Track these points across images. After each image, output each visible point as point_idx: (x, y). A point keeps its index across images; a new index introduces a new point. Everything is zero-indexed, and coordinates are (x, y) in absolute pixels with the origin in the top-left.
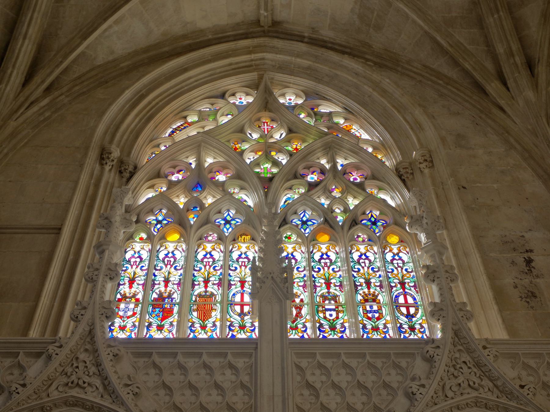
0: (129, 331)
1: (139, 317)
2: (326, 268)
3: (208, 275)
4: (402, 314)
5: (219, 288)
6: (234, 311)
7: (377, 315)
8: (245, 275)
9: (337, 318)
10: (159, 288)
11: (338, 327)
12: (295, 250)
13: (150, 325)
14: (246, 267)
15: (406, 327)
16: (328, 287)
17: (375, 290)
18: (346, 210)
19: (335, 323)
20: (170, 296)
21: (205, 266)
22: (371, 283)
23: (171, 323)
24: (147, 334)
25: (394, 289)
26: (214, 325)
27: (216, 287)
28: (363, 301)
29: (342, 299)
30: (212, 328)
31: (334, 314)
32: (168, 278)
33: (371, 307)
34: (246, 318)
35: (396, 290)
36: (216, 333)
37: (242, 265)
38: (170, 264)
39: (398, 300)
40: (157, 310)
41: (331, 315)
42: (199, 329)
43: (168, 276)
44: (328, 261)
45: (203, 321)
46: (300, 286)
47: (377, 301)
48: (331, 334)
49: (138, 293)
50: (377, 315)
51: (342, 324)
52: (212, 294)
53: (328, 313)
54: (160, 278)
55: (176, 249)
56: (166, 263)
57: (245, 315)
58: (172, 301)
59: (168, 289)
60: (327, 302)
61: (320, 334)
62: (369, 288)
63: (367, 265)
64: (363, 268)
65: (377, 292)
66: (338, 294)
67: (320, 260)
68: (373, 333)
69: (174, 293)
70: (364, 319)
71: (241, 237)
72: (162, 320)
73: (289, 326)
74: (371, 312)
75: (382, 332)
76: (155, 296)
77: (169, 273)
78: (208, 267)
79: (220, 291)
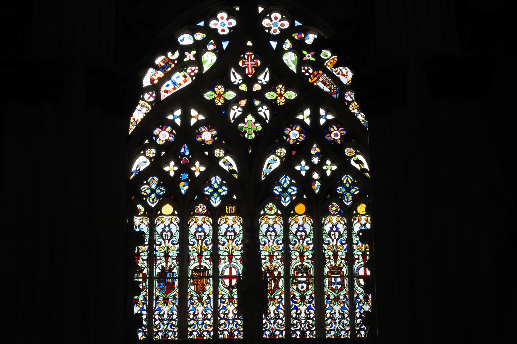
0: (141, 304)
1: (147, 291)
2: (301, 241)
3: (201, 250)
4: (360, 285)
6: (224, 284)
7: (339, 287)
8: (232, 249)
9: (307, 289)
10: (160, 263)
11: (307, 297)
12: (275, 222)
13: (157, 298)
14: (233, 240)
15: (361, 297)
16: (302, 260)
17: (341, 262)
20: (171, 270)
21: (198, 240)
22: (338, 255)
23: (174, 296)
24: (156, 306)
25: (357, 261)
26: (209, 298)
27: (208, 261)
30: (207, 301)
32: (168, 253)
33: (336, 279)
34: (234, 290)
35: (358, 263)
36: (211, 305)
37: (229, 239)
39: (358, 272)
40: (162, 284)
41: (302, 287)
42: (197, 301)
43: (167, 251)
44: (303, 233)
45: (200, 294)
46: (278, 259)
48: (301, 304)
49: (144, 268)
50: (339, 287)
51: (311, 295)
52: (206, 269)
53: (300, 285)
54: (160, 254)
55: (171, 222)
57: (233, 288)
58: (173, 275)
59: (169, 264)
60: (300, 275)
61: (292, 305)
62: (335, 261)
63: (337, 237)
64: (333, 240)
65: (342, 265)
66: (310, 266)
67: (296, 232)
69: (174, 268)
70: (329, 290)
71: (228, 208)
72: (167, 294)
73: (268, 297)
75: (341, 302)
76: (158, 271)
77: (168, 248)
78: (200, 241)
79: (212, 266)
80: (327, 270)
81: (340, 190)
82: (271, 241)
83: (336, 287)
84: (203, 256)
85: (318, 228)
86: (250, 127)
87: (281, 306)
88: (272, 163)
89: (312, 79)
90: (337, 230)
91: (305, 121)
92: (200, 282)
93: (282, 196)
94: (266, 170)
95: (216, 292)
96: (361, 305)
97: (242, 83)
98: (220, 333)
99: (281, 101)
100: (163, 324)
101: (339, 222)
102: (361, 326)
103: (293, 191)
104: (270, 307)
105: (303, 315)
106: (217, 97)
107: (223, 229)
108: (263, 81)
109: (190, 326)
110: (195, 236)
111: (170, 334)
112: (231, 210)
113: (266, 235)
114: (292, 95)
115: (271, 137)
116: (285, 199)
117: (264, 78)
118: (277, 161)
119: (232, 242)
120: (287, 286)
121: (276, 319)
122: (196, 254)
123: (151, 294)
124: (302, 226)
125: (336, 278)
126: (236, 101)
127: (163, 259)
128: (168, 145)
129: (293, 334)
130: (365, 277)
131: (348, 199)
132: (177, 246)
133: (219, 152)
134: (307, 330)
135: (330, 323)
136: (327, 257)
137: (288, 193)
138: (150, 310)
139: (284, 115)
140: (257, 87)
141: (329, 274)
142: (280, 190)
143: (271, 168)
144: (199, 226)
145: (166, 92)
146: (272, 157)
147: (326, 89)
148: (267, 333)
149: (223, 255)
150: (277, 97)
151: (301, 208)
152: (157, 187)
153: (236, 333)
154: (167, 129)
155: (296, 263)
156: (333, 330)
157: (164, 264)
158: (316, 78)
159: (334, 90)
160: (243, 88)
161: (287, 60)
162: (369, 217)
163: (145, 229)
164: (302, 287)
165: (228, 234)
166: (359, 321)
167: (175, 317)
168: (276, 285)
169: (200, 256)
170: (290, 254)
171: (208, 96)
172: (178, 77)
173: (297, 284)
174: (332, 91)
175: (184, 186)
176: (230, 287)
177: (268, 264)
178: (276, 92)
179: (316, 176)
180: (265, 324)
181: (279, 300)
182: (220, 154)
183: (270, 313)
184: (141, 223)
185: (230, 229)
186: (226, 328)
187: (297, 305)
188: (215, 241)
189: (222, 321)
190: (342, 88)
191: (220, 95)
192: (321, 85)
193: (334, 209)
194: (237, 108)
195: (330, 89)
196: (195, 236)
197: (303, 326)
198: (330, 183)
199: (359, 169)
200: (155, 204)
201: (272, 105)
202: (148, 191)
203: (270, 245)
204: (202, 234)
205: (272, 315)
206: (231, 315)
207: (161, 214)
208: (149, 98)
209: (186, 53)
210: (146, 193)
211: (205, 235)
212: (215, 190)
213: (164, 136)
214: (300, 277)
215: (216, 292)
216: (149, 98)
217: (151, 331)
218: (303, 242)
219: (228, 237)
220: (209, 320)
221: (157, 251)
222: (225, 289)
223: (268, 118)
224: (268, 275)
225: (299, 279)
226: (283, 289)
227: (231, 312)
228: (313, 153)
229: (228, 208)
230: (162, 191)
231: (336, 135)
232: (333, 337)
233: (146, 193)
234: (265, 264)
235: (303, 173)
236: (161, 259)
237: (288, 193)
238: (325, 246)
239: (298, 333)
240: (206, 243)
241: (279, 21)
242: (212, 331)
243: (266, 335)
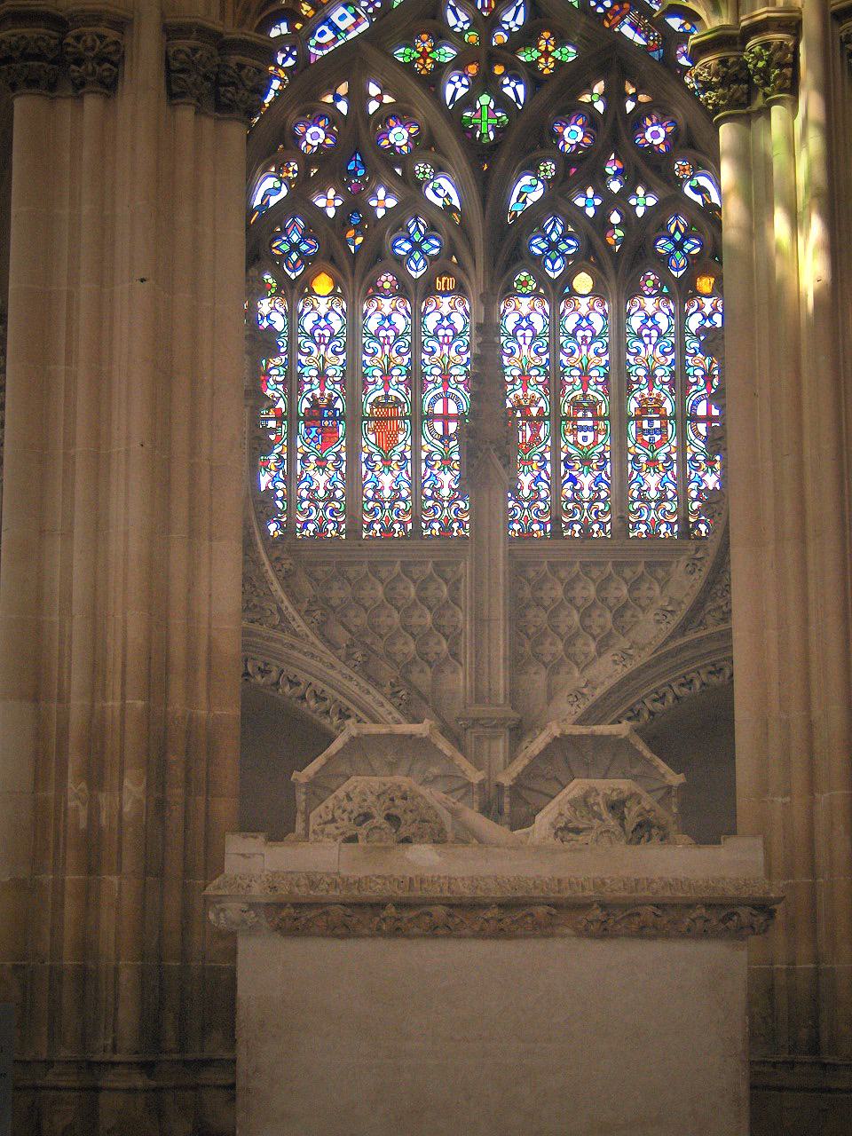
0: (273, 468)
1: (285, 443)
2: (584, 348)
4: (698, 435)
5: (407, 390)
7: (657, 438)
9: (595, 443)
10: (311, 390)
13: (305, 458)
14: (450, 345)
16: (585, 386)
18: (628, 220)
19: (590, 452)
20: (330, 406)
21: (383, 346)
27: (402, 387)
28: (638, 413)
29: (603, 410)
30: (399, 464)
31: (590, 435)
32: (324, 371)
34: (452, 444)
35: (697, 391)
38: (324, 343)
40: (314, 430)
41: (585, 439)
47: (662, 412)
50: (657, 438)
53: (580, 435)
55: (331, 309)
56: (317, 339)
58: (335, 414)
59: (327, 392)
61: (566, 472)
64: (646, 346)
66: (600, 398)
67: (575, 330)
68: (648, 470)
71: (441, 280)
73: (519, 457)
74: (649, 432)
76: (306, 404)
77: (324, 360)
78: (387, 348)
79: (409, 396)
80: (633, 405)
81: (664, 246)
82: (525, 348)
83: (651, 439)
84: (392, 376)
85: (619, 320)
86: (486, 118)
87: (544, 476)
88: (527, 191)
89: (609, 21)
90: (655, 327)
91: (596, 105)
92: (386, 427)
93: (549, 257)
94: (515, 206)
95: (416, 448)
96: (701, 473)
97: (468, 31)
98: (424, 525)
100: (317, 507)
101: (659, 309)
102: (699, 516)
103: (570, 247)
104: (522, 477)
105: (586, 493)
106: (419, 58)
107: (431, 322)
108: (512, 24)
109: (369, 512)
110: (375, 337)
111: (330, 526)
112: (446, 283)
113: (515, 336)
114: (569, 54)
115: (527, 139)
116: (553, 263)
117: (514, 19)
118: (538, 187)
119: (449, 349)
120: (556, 434)
121: (533, 501)
122: (378, 373)
123: (292, 449)
124: (587, 318)
125: (651, 420)
126: (459, 64)
127: (316, 381)
128: (321, 156)
129: (566, 529)
130: (708, 419)
131: (677, 263)
132: (343, 357)
133: (422, 170)
134: (594, 523)
135: (639, 509)
136: (634, 379)
137: (559, 252)
138: (291, 479)
139: (557, 94)
140: (500, 38)
141: (638, 413)
142: (543, 246)
143: (525, 202)
144: (384, 318)
145: (319, 46)
146: (526, 180)
147: (639, 40)
148: (516, 527)
149: (432, 375)
150: (539, 58)
151: (583, 282)
152: (303, 239)
153: (455, 525)
154: (322, 124)
155: (573, 391)
156: (645, 523)
157: (317, 392)
158: (618, 18)
160: (472, 37)
162: (720, 303)
163: (280, 323)
164: (585, 439)
165: (441, 332)
166: (696, 505)
167: (339, 494)
168: (535, 435)
169: (386, 376)
170: (563, 374)
171: (402, 54)
172: (343, 17)
173: (574, 432)
174: (652, 43)
175: (355, 237)
176: (445, 437)
177: (520, 392)
178: (537, 47)
179: (615, 218)
180: (513, 509)
181: (540, 464)
182: (424, 173)
183: (522, 488)
184: (272, 312)
185: (446, 323)
186: (437, 516)
187: (574, 473)
188: (416, 347)
189: (430, 503)
191: (424, 55)
192: (627, 31)
193: (650, 283)
194: (460, 80)
195: (646, 39)
196: (375, 337)
197: (586, 514)
198: (643, 233)
199: (701, 204)
200: (298, 273)
201: (531, 75)
202: (285, 247)
203: (520, 356)
204: (391, 333)
205: (526, 493)
206: (445, 492)
207: (312, 292)
208: (285, 60)
210: (280, 250)
211: (396, 336)
212: (417, 246)
213: (315, 136)
214: (580, 419)
215: (416, 448)
216: (285, 60)
217: (292, 521)
218: (588, 350)
219: (441, 338)
220: (405, 501)
221: (303, 366)
222: (435, 441)
223: (522, 101)
224: (519, 415)
225: (580, 423)
226: (549, 443)
227: (446, 486)
228: (609, 171)
229: (441, 280)
230: (311, 247)
231: (655, 135)
232: (644, 536)
233: (280, 250)
234: (515, 393)
235: (590, 212)
236: (311, 382)
237: (559, 252)
238: (631, 358)
239: (577, 527)
240: (398, 352)
242: (411, 521)
243: (513, 530)
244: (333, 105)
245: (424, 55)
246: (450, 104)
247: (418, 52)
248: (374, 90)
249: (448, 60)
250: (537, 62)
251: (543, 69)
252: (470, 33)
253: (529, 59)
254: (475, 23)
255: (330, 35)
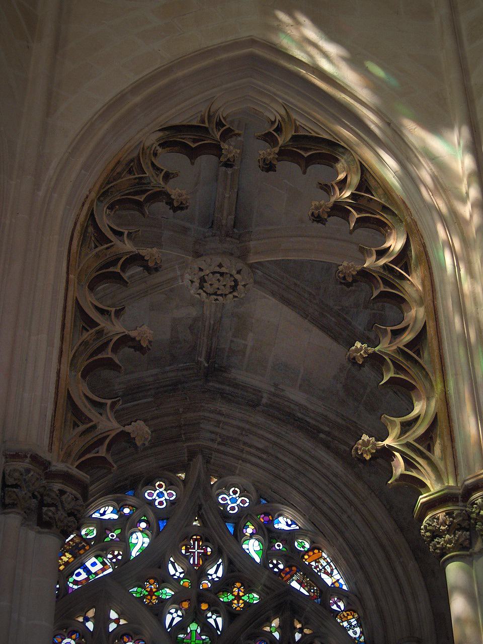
97: (183, 578)
99: (238, 605)
106: (147, 595)
108: (214, 576)
117: (216, 573)
126: (176, 600)
140: (206, 584)
145: (75, 582)
150: (233, 600)
154: (74, 636)
158: (288, 576)
159: (314, 592)
160: (186, 583)
161: (248, 549)
172: (94, 564)
174: (312, 594)
178: (232, 593)
190: (326, 592)
191: (151, 593)
192: (295, 584)
194: (176, 612)
209: (107, 532)
241: (239, 497)
244: (83, 623)
245: (151, 593)
246: (169, 627)
247: (147, 591)
248: (113, 615)
249: (168, 597)
250: (231, 603)
251: (236, 608)
252: (184, 580)
253: (225, 600)
254: (187, 574)
255: (84, 576)
